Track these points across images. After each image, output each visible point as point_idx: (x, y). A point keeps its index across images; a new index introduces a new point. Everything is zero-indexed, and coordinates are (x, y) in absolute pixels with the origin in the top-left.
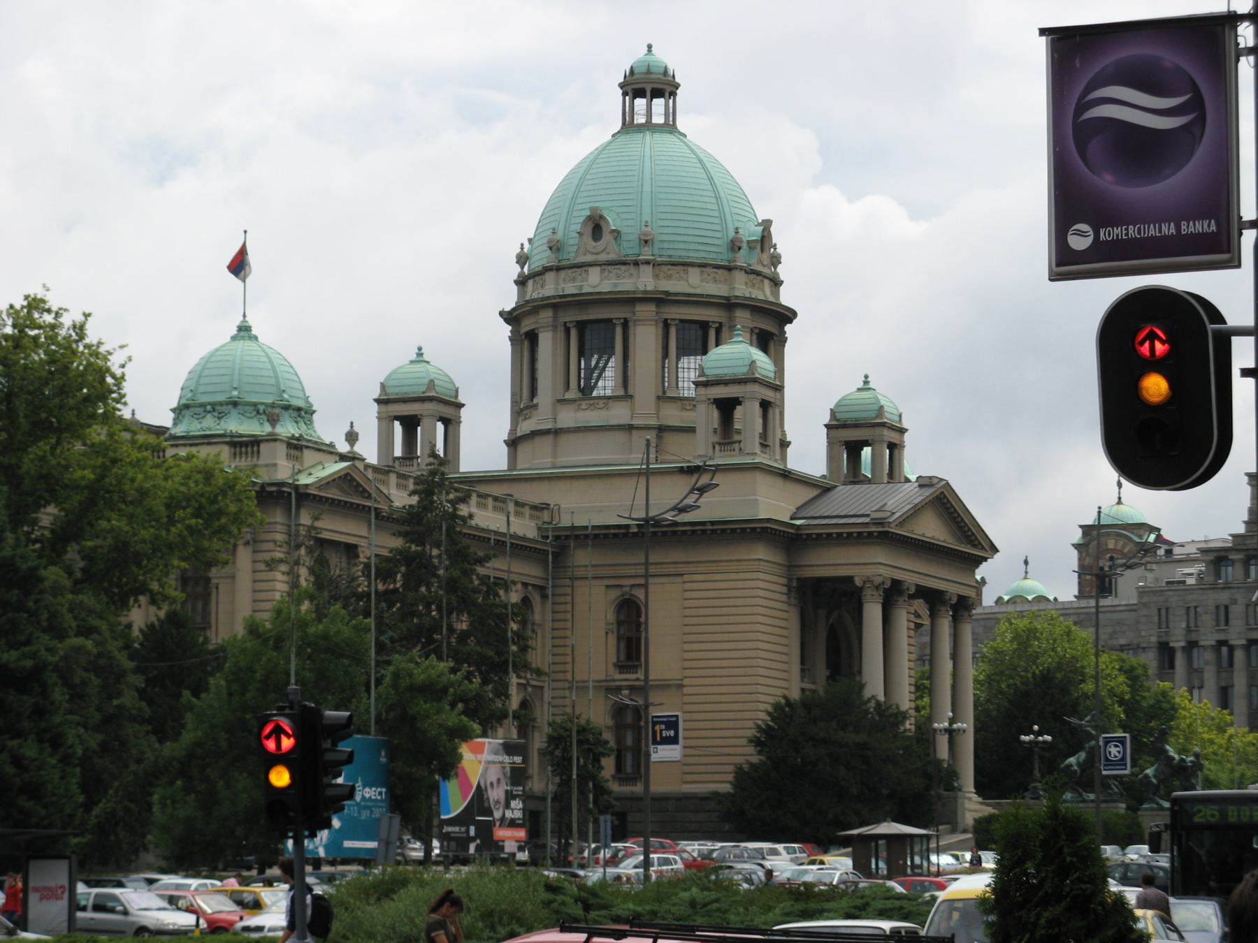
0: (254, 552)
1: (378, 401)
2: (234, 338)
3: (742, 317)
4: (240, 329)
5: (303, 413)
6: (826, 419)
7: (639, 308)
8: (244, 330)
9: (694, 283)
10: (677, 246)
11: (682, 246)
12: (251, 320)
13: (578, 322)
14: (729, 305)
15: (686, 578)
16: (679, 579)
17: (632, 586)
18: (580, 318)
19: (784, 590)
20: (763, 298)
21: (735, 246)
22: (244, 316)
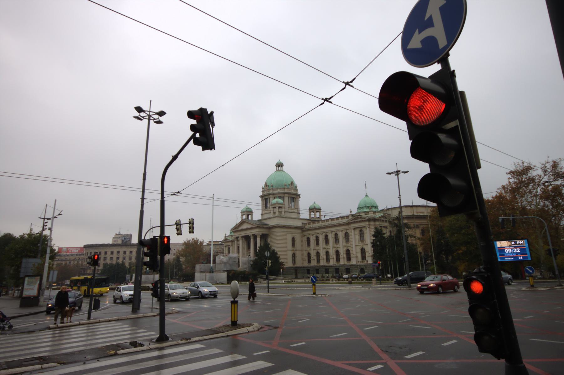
4: (366, 196)
8: (367, 196)
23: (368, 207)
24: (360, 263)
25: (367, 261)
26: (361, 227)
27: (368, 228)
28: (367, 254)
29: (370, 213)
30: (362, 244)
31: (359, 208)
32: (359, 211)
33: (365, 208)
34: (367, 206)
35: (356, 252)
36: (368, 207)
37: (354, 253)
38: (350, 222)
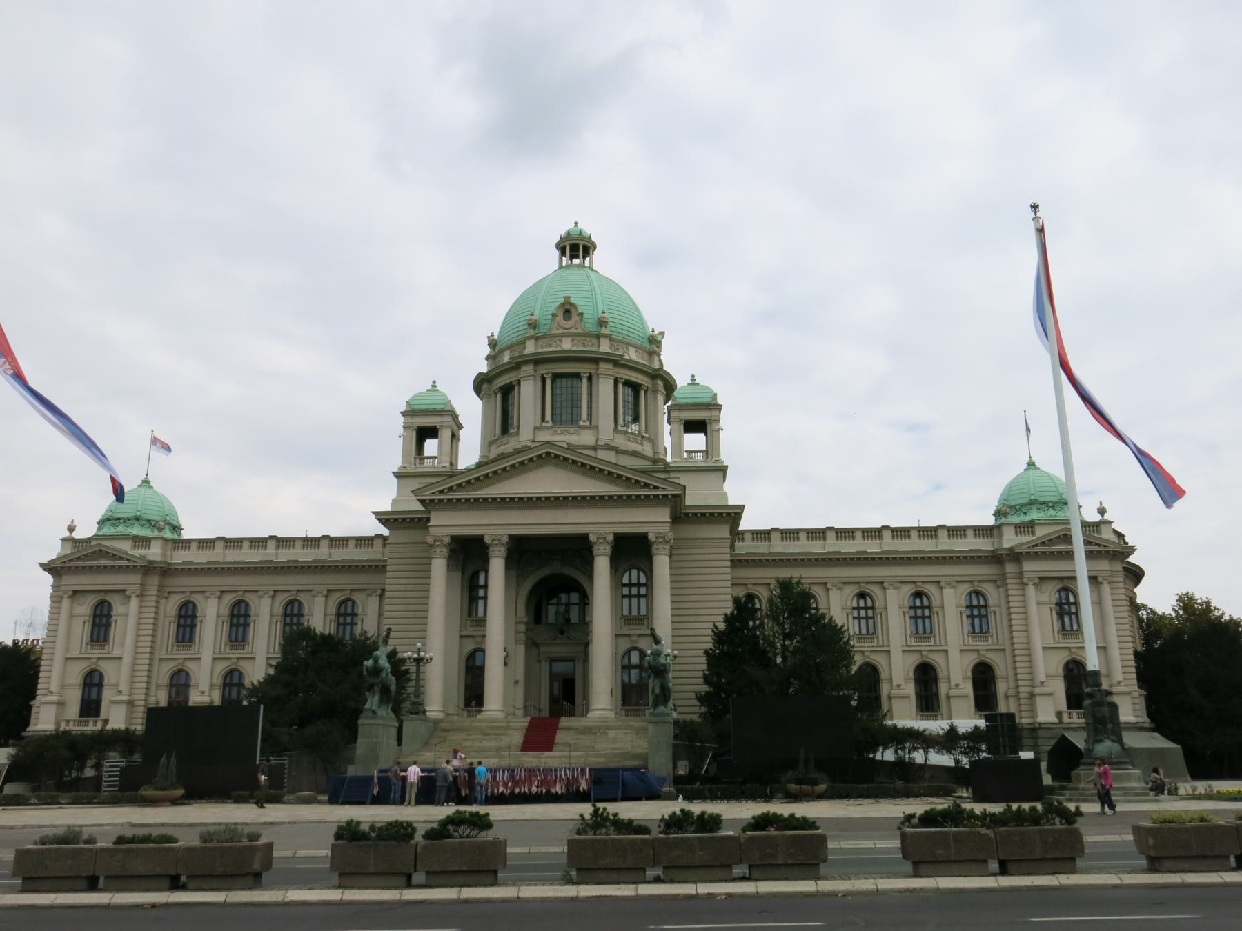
0: (141, 601)
2: (140, 486)
3: (528, 369)
4: (144, 482)
5: (122, 521)
12: (150, 478)
14: (516, 366)
20: (558, 349)
21: (533, 325)
22: (147, 475)
23: (151, 524)
24: (72, 727)
25: (106, 721)
26: (106, 591)
27: (138, 596)
28: (107, 695)
29: (153, 542)
30: (96, 653)
31: (102, 523)
32: (108, 530)
33: (136, 522)
34: (145, 516)
35: (63, 686)
37: (54, 687)
38: (62, 568)
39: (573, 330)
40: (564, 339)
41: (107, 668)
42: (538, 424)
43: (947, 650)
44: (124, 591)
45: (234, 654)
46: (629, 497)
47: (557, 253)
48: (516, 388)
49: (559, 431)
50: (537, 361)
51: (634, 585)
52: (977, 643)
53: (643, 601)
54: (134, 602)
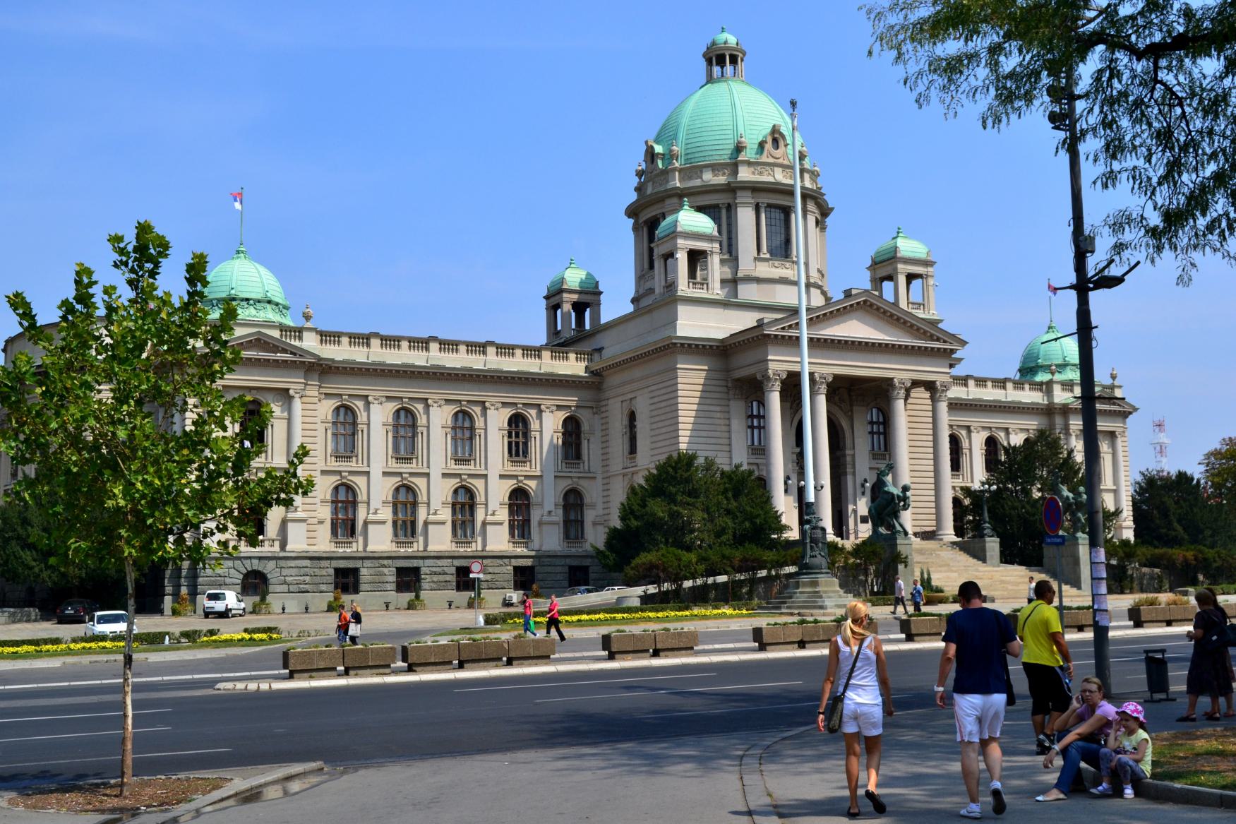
1: (547, 298)
3: (744, 197)
5: (251, 302)
6: (869, 263)
7: (668, 202)
9: (708, 177)
10: (697, 155)
11: (700, 154)
13: (645, 222)
14: (732, 189)
15: (650, 389)
16: (646, 390)
17: (631, 399)
18: (644, 219)
19: (725, 389)
20: (771, 179)
29: (305, 334)
33: (268, 306)
36: (277, 304)
39: (781, 161)
40: (776, 169)
41: (584, 486)
42: (756, 255)
43: (368, 473)
44: (288, 390)
45: (407, 468)
46: (926, 348)
47: (703, 63)
48: (724, 212)
49: (776, 263)
50: (755, 188)
51: (875, 423)
52: (570, 470)
53: (882, 437)
54: (297, 405)
